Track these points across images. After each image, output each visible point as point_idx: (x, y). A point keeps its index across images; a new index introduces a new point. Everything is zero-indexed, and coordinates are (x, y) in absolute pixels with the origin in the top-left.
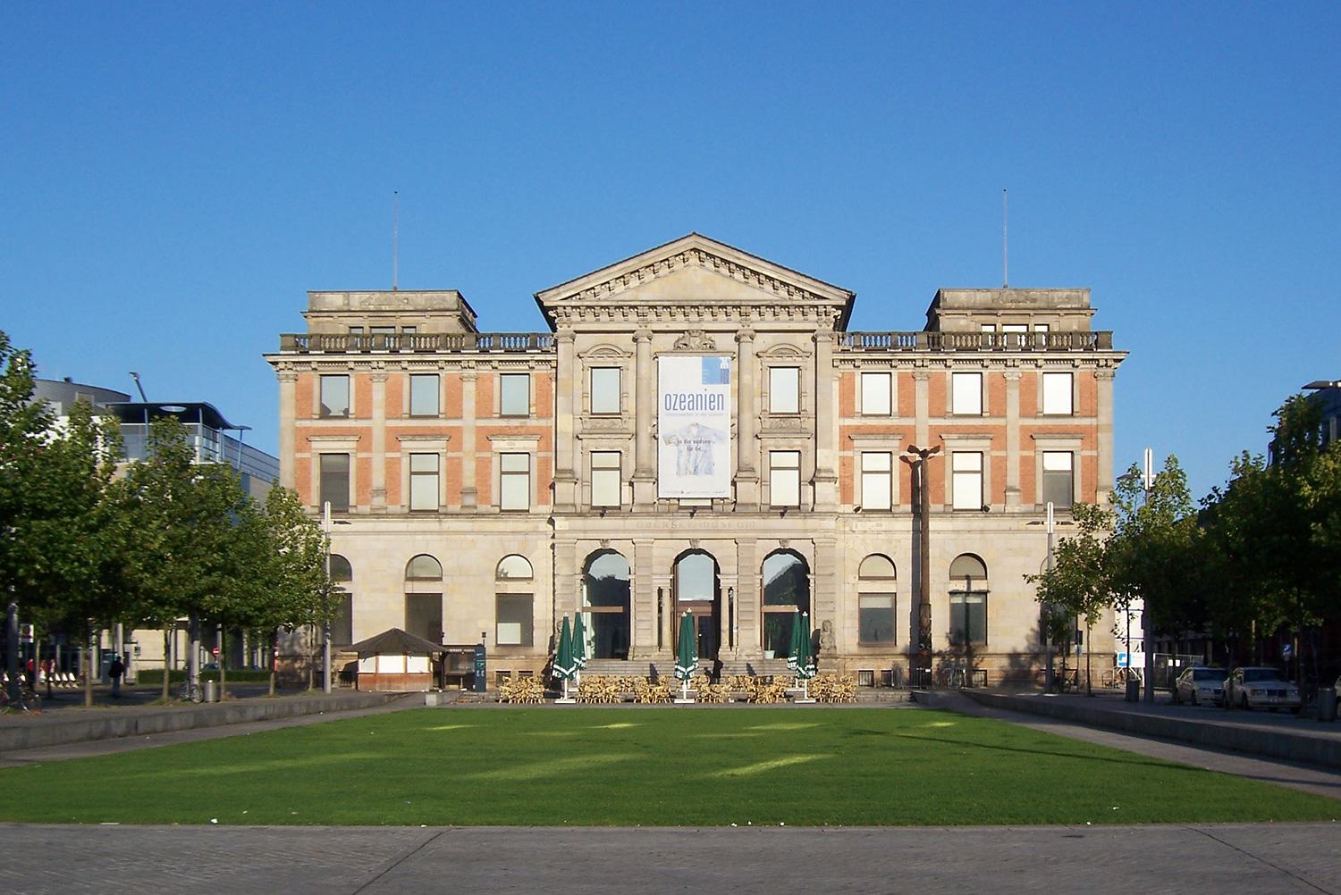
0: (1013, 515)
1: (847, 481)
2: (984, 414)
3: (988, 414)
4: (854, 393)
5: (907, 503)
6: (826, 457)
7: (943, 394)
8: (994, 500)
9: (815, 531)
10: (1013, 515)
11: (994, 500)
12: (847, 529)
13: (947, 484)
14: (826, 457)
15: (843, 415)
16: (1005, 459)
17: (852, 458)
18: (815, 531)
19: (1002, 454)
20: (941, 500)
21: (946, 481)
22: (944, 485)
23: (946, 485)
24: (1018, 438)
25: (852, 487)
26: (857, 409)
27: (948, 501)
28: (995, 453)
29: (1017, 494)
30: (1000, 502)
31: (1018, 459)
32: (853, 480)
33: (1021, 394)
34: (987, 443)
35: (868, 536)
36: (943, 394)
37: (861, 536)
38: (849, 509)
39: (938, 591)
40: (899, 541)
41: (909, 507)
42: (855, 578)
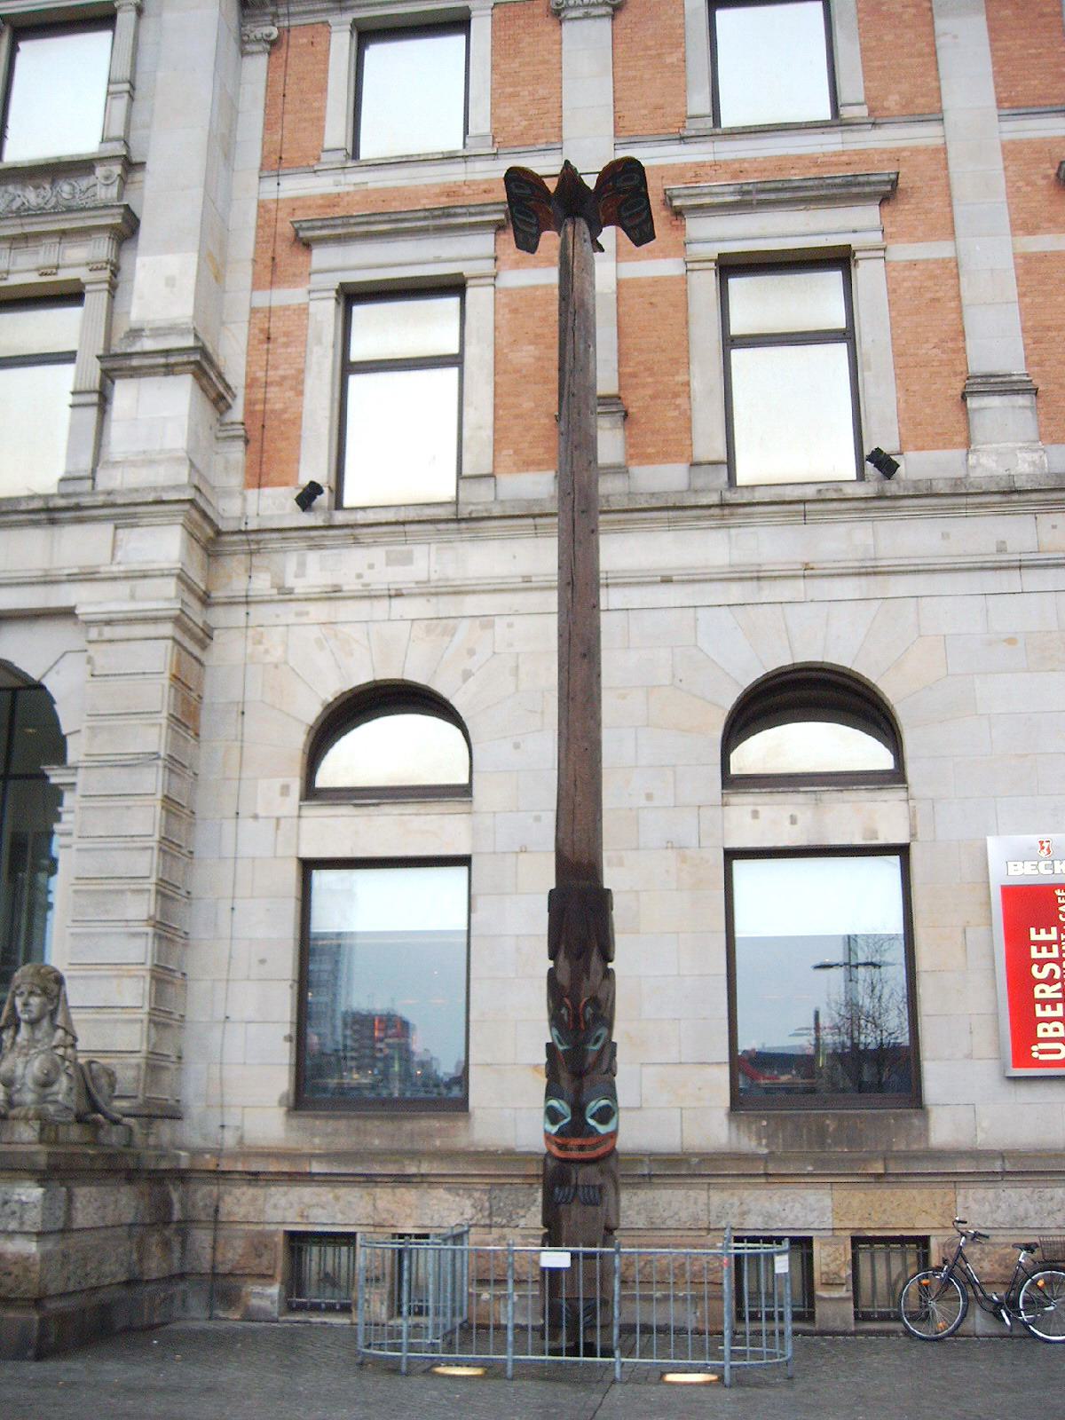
0: (1009, 495)
1: (277, 398)
2: (846, 113)
3: (861, 112)
4: (323, 89)
5: (528, 465)
6: (170, 282)
7: (672, 59)
8: (918, 432)
9: (88, 576)
10: (1009, 495)
11: (918, 432)
12: (262, 584)
13: (704, 377)
14: (170, 282)
15: (275, 164)
16: (952, 270)
17: (303, 311)
18: (88, 576)
19: (939, 250)
20: (676, 444)
21: (695, 368)
22: (688, 384)
23: (696, 385)
24: (1001, 184)
25: (296, 422)
26: (335, 133)
27: (709, 445)
28: (902, 252)
29: (1022, 400)
30: (940, 440)
31: (1007, 265)
32: (301, 393)
33: (995, 31)
34: (868, 215)
35: (347, 610)
36: (672, 59)
37: (318, 611)
38: (276, 505)
39: (670, 845)
40: (486, 621)
41: (539, 485)
42: (285, 790)
